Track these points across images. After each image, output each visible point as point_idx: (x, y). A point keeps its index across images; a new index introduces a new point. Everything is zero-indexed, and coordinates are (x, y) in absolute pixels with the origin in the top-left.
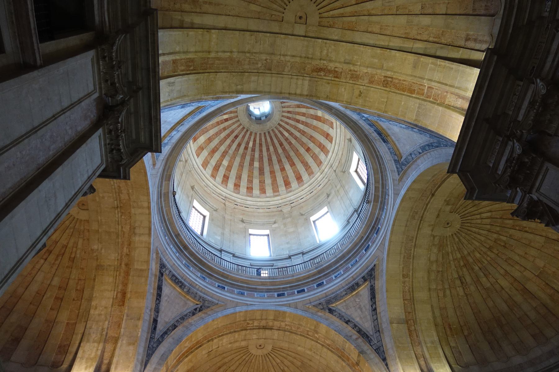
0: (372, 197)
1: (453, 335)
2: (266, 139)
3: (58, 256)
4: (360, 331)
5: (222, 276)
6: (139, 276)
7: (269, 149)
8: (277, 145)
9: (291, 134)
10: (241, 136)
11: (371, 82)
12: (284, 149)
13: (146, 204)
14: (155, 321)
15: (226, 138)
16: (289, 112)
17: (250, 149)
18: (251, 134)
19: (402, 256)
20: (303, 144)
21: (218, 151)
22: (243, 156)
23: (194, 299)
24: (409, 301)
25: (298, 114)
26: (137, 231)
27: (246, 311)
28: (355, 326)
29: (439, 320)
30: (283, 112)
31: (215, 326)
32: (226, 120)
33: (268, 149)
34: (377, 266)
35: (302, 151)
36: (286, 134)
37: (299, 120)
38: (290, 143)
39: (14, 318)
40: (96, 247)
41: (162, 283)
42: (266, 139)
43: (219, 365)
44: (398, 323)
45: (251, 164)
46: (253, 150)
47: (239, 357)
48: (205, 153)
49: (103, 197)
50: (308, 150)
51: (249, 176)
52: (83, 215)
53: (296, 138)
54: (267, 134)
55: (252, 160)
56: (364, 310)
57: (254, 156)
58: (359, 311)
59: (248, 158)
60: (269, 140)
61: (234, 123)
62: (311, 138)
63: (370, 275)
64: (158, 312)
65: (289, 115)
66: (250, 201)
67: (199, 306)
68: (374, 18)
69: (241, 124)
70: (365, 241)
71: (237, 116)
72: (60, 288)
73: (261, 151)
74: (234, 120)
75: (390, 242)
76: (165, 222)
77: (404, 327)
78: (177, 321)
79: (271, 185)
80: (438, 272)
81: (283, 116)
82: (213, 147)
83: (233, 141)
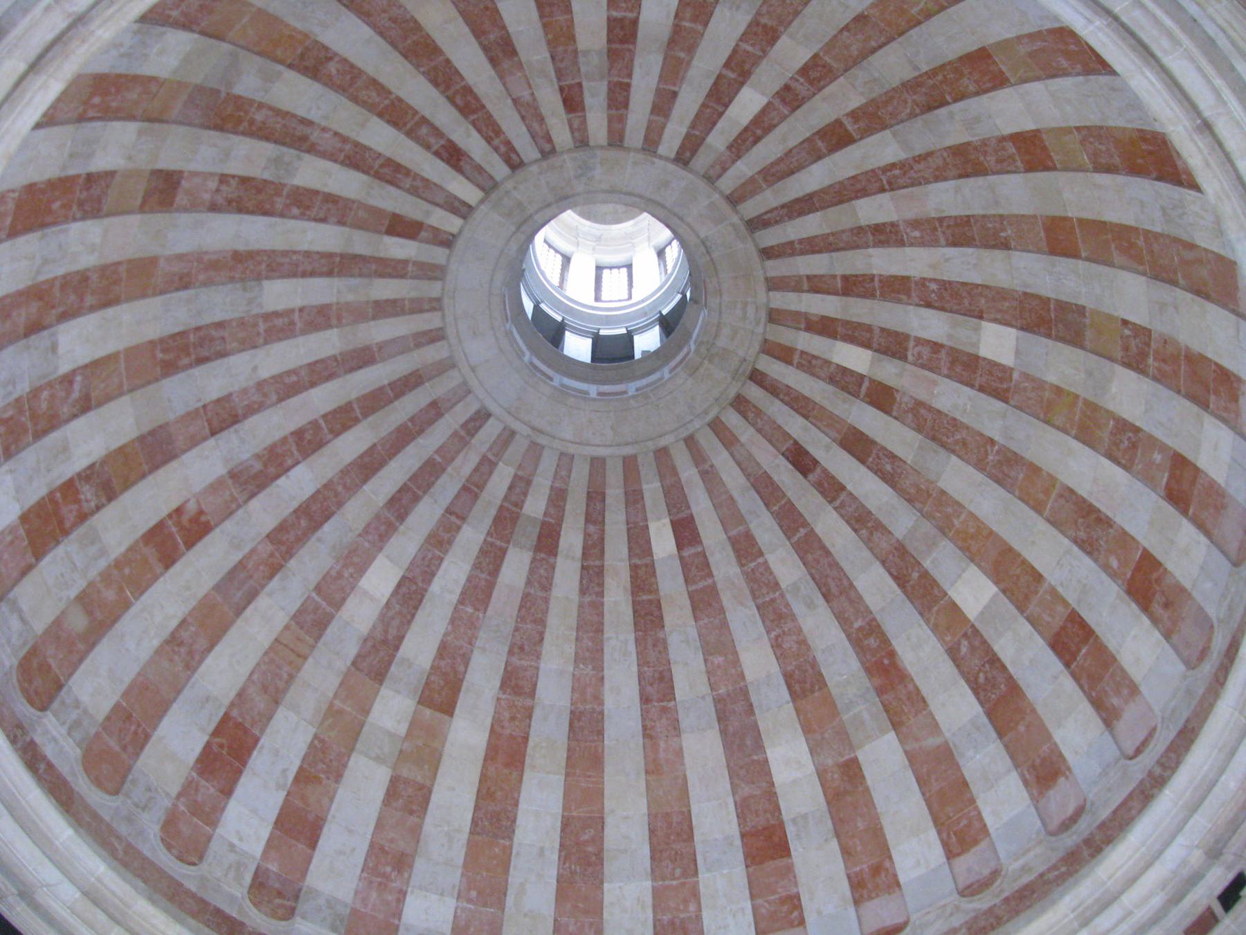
2: (812, 246)
7: (878, 229)
10: (796, 426)
12: (872, 118)
15: (809, 547)
16: (572, 102)
17: (889, 372)
18: (784, 354)
21: (890, 626)
22: (939, 429)
30: (582, 142)
32: (685, 531)
33: (885, 235)
36: (748, 103)
37: (613, 24)
38: (816, 73)
42: (812, 246)
45: (994, 382)
46: (893, 345)
51: (1086, 435)
54: (771, 237)
55: (969, 368)
57: (936, 347)
59: (951, 397)
60: (811, 225)
61: (709, 476)
69: (717, 426)
71: (662, 455)
73: (896, 288)
74: (688, 473)
79: (1164, 292)
81: (616, 139)
82: (854, 664)
83: (831, 489)
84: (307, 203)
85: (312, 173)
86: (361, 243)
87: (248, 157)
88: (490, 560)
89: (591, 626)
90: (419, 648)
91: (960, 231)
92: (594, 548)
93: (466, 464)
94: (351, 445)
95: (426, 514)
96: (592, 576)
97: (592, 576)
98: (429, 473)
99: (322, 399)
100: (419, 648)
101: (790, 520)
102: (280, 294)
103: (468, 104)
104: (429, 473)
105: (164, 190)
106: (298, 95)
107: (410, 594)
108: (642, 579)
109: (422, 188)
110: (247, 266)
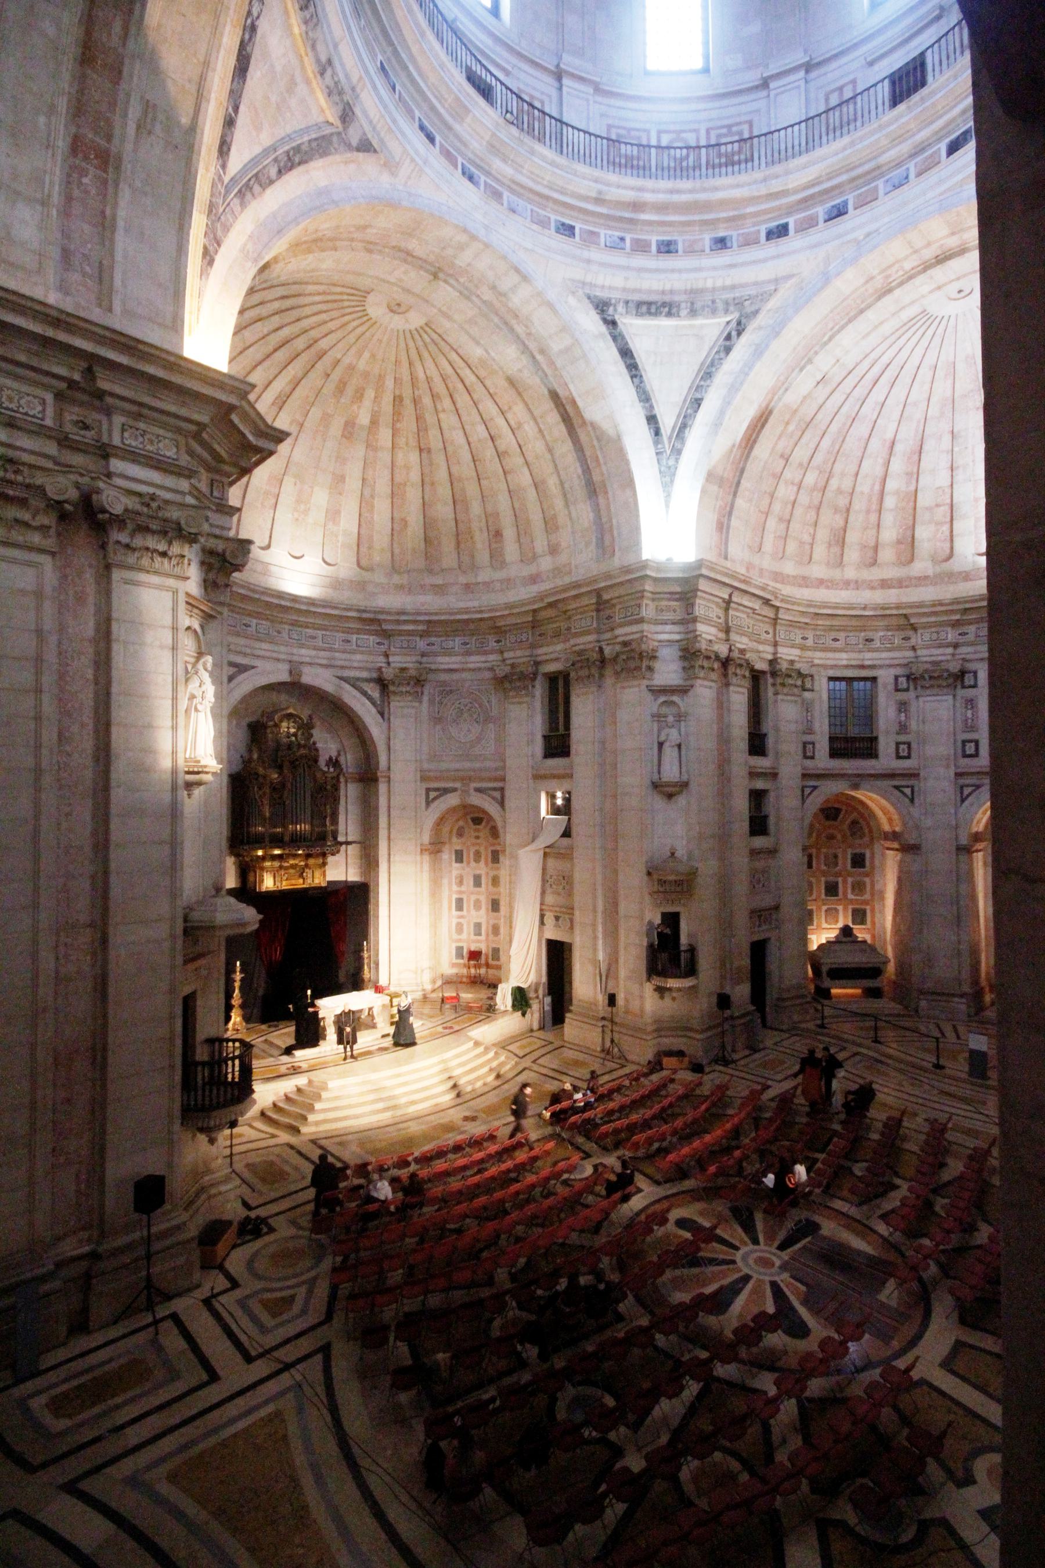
13: (463, 238)
14: (652, 419)
39: (476, 508)
40: (479, 352)
41: (623, 338)
49: (401, 280)
52: (415, 320)
67: (733, 324)
76: (547, 198)
78: (699, 388)
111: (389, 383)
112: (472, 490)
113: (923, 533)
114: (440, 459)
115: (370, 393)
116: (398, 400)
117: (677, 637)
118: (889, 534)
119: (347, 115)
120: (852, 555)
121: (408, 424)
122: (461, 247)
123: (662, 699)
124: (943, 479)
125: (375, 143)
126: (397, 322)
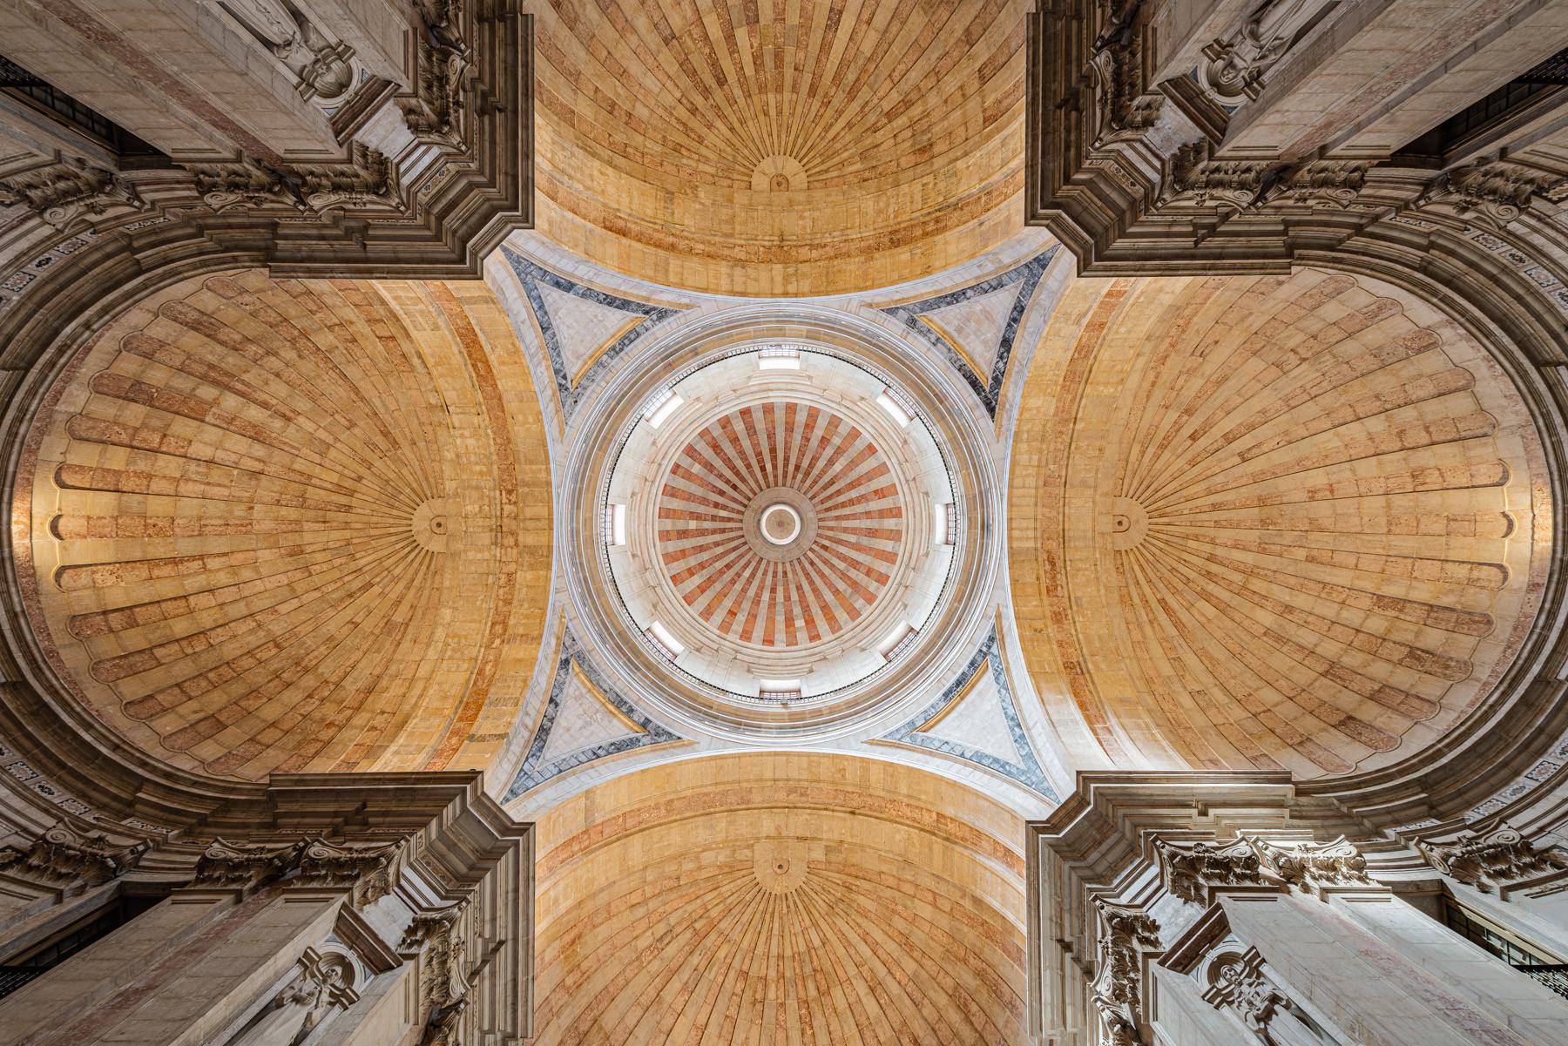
0: (796, 707)
1: (563, 950)
3: (685, 125)
4: (543, 733)
5: (605, 438)
6: (656, 265)
8: (727, 560)
9: (749, 582)
10: (736, 495)
11: (1060, 644)
12: (721, 572)
13: (792, 288)
14: (570, 287)
15: (733, 468)
16: (785, 573)
18: (739, 512)
19: (710, 789)
20: (738, 603)
22: (704, 501)
23: (584, 375)
24: (626, 829)
25: (787, 590)
26: (738, 271)
27: (549, 484)
28: (552, 720)
29: (589, 907)
31: (520, 417)
32: (763, 469)
33: (717, 544)
34: (679, 743)
35: (728, 603)
38: (733, 582)
43: (396, 433)
44: (587, 810)
46: (714, 518)
47: (410, 478)
48: (717, 432)
49: (802, 218)
50: (732, 613)
52: (760, 182)
53: (744, 590)
55: (698, 517)
56: (586, 733)
58: (580, 723)
59: (701, 509)
61: (757, 481)
62: (753, 617)
63: (656, 734)
64: (583, 296)
65: (780, 574)
66: (653, 511)
68: (1148, 629)
70: (706, 714)
72: (630, 115)
73: (714, 532)
74: (762, 482)
75: (740, 756)
77: (577, 826)
80: (678, 878)
83: (727, 482)
84: (844, 559)
85: (842, 566)
86: (834, 546)
87: (853, 573)
88: (811, 466)
89: (787, 448)
90: (829, 452)
91: (701, 549)
92: (786, 465)
93: (817, 488)
94: (842, 499)
95: (826, 479)
96: (787, 459)
97: (787, 459)
98: (825, 488)
99: (847, 511)
100: (829, 451)
101: (737, 474)
102: (853, 539)
103: (807, 575)
104: (825, 488)
105: (869, 572)
106: (841, 585)
107: (831, 462)
108: (774, 458)
109: (820, 557)
110: (857, 547)
111: (738, 92)
112: (607, 33)
113: (134, 413)
114: (653, 40)
115: (749, 70)
116: (721, 81)
117: (403, 168)
118: (157, 376)
119: (912, 323)
120: (163, 329)
121: (698, 61)
122: (786, 279)
123: (355, 84)
124: (197, 450)
125: (884, 315)
126: (767, 165)
